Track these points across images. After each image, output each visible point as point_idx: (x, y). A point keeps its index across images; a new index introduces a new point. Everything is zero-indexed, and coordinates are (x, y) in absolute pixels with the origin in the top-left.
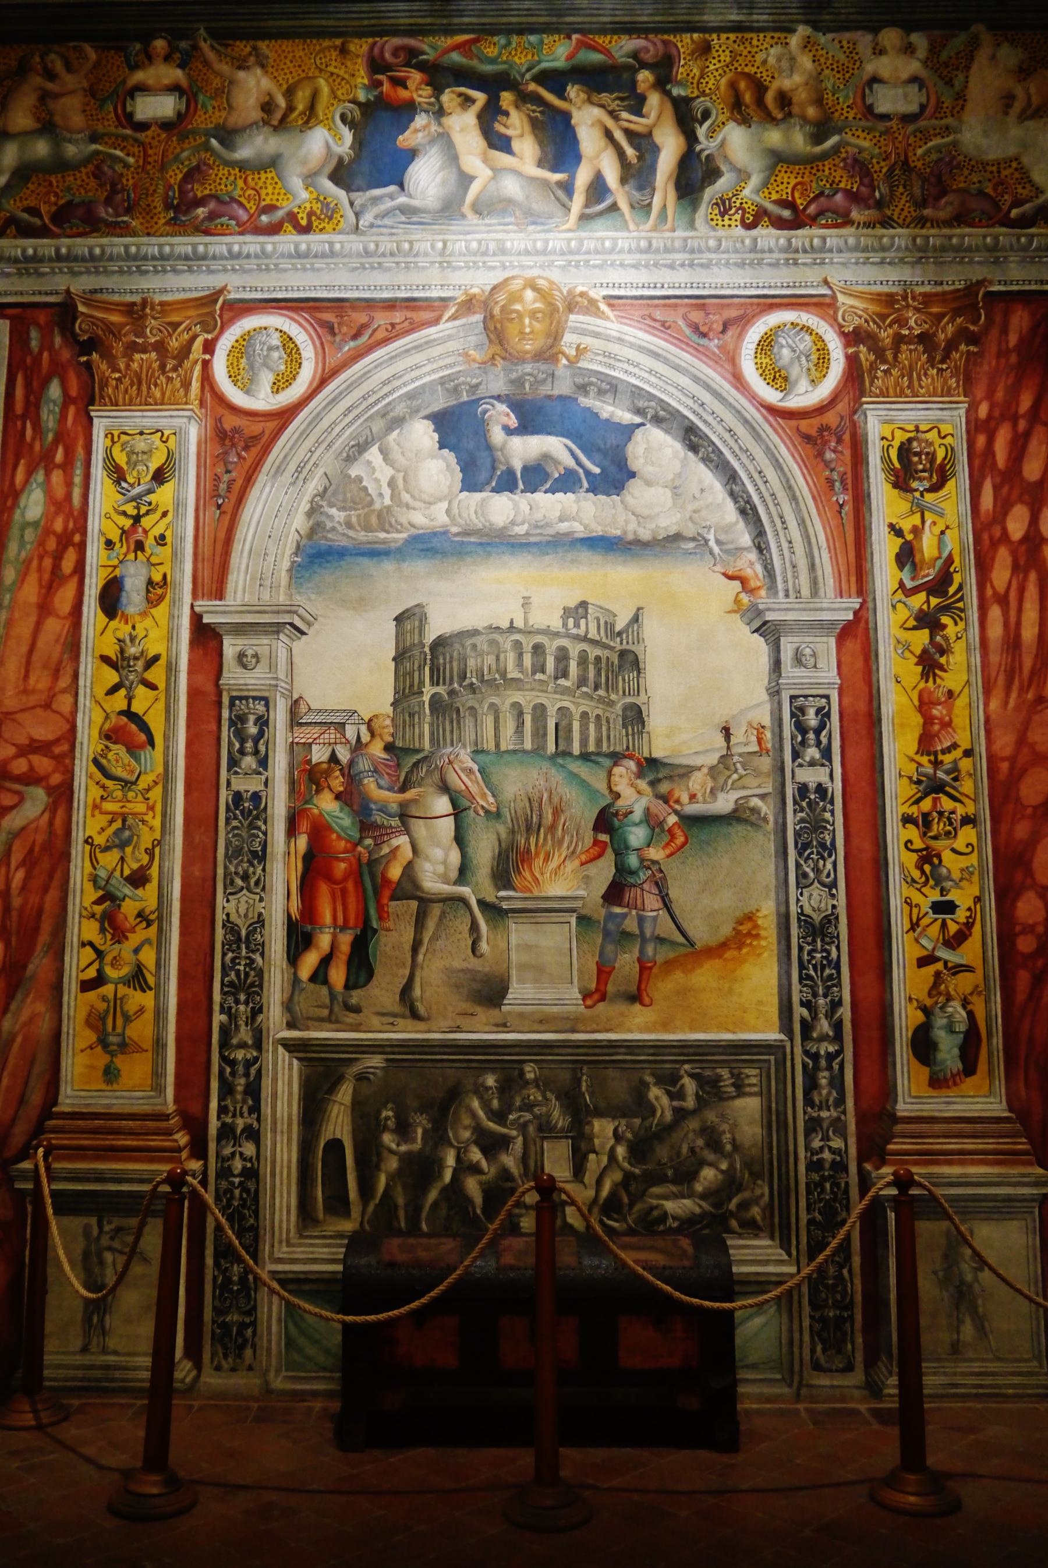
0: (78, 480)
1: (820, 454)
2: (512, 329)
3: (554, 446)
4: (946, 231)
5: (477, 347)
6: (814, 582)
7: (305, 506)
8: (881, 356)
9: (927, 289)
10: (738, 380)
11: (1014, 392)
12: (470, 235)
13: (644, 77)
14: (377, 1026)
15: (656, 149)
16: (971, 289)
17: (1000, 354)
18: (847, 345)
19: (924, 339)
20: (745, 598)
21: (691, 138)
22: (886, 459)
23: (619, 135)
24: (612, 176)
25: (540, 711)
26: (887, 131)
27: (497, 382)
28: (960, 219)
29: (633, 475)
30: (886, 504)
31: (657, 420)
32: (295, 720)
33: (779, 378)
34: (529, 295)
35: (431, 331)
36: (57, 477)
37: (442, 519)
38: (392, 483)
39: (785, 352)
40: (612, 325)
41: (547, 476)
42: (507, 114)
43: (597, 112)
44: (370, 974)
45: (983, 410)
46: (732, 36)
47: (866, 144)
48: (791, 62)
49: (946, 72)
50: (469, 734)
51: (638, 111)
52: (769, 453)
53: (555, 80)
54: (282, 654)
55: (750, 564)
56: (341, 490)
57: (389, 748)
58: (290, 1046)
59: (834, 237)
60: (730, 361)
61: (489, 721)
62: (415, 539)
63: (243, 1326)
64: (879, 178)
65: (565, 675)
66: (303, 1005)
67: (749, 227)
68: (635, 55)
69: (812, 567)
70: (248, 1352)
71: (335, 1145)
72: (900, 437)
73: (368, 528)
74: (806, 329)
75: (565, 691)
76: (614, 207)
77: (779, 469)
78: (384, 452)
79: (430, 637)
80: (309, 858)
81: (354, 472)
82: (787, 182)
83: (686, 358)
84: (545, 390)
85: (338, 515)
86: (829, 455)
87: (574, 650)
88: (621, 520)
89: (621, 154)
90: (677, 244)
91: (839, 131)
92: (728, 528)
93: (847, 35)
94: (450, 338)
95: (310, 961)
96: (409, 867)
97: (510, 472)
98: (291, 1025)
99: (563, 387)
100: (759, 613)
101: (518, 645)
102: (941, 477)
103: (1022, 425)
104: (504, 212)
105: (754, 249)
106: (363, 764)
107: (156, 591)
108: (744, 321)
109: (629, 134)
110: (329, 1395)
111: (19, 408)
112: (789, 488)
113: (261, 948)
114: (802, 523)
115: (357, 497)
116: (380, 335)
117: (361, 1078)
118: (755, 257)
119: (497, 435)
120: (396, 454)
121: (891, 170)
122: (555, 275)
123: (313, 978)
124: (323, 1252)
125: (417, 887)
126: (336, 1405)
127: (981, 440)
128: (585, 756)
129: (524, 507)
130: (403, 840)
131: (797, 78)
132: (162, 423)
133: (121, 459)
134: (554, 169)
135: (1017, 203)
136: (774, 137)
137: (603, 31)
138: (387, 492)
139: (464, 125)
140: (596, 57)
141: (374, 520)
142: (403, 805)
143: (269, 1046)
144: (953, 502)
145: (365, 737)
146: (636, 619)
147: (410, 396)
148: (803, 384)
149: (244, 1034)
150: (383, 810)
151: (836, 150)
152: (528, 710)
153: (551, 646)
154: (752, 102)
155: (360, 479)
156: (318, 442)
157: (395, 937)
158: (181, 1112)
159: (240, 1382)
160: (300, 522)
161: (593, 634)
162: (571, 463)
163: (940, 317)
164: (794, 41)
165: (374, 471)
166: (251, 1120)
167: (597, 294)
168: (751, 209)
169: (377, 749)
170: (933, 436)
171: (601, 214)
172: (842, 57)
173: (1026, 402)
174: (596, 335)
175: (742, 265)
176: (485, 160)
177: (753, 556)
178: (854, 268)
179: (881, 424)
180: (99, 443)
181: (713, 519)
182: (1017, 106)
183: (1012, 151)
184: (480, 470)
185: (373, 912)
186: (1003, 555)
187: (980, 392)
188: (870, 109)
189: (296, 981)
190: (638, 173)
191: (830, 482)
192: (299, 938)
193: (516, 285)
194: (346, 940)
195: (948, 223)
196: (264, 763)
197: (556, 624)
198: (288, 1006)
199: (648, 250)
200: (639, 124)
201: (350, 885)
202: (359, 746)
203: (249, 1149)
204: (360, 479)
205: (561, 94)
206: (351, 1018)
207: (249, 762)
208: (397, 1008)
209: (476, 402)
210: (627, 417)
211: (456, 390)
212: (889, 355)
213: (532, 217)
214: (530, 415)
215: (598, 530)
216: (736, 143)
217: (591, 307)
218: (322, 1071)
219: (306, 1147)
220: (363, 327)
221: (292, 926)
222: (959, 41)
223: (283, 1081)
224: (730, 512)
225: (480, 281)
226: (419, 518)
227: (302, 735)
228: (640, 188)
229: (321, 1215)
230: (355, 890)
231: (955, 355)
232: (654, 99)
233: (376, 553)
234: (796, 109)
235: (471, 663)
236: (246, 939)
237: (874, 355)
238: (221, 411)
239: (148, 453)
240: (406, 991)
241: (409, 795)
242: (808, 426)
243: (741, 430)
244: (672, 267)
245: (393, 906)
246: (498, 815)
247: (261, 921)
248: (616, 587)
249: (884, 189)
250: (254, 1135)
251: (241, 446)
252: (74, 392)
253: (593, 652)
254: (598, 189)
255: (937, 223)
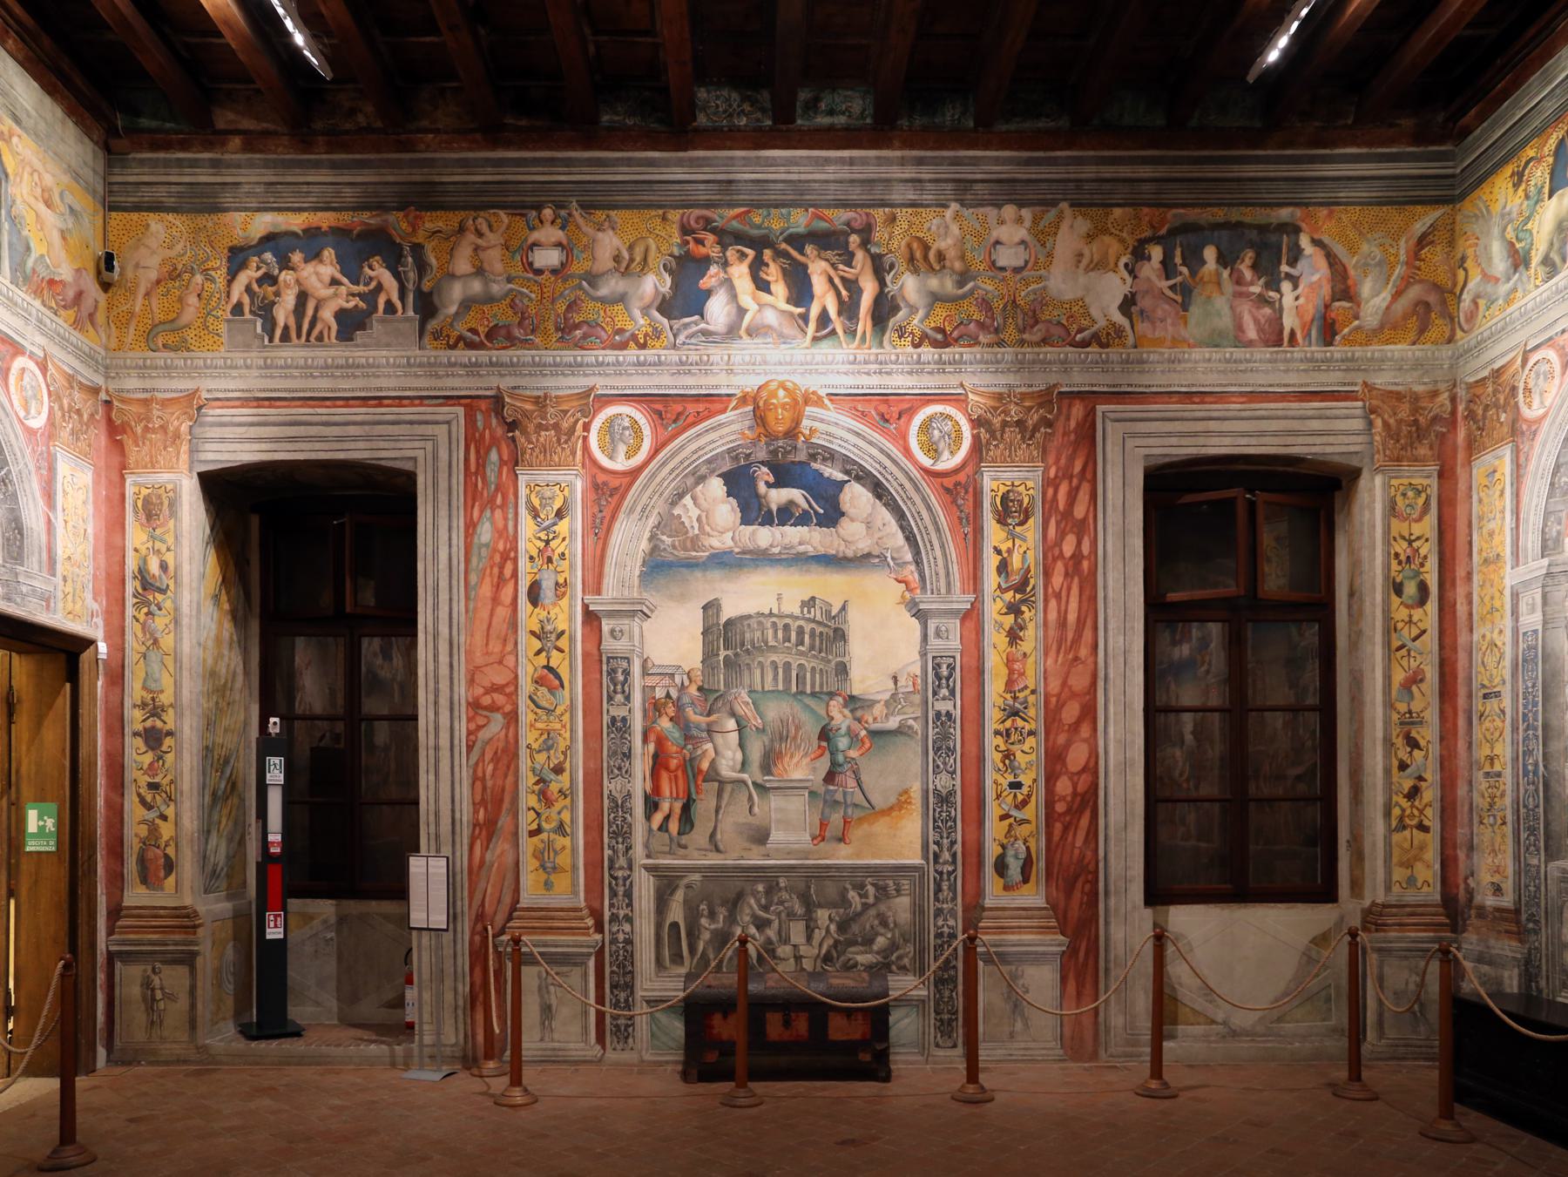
0: (511, 516)
1: (954, 501)
2: (770, 417)
3: (796, 494)
4: (1036, 350)
5: (750, 428)
6: (949, 584)
7: (647, 535)
8: (992, 434)
9: (1023, 389)
10: (907, 452)
11: (1071, 459)
12: (744, 350)
13: (854, 239)
14: (696, 856)
15: (860, 291)
16: (1049, 390)
17: (1064, 434)
18: (973, 428)
19: (1020, 423)
20: (908, 595)
21: (882, 283)
22: (993, 504)
23: (837, 281)
24: (832, 312)
25: (787, 666)
26: (1004, 279)
27: (762, 455)
28: (1045, 341)
29: (843, 514)
30: (994, 534)
31: (858, 479)
32: (645, 672)
33: (933, 450)
34: (781, 393)
35: (722, 418)
36: (498, 513)
37: (730, 543)
38: (699, 519)
39: (936, 432)
40: (831, 414)
41: (792, 515)
42: (767, 265)
43: (824, 264)
44: (692, 826)
45: (1052, 473)
46: (910, 210)
47: (990, 288)
48: (946, 228)
49: (1043, 235)
50: (746, 681)
51: (849, 264)
52: (924, 500)
53: (797, 241)
54: (636, 630)
55: (911, 572)
56: (669, 523)
57: (700, 689)
58: (648, 868)
59: (967, 353)
60: (901, 439)
61: (758, 672)
62: (713, 557)
63: (627, 1026)
64: (998, 312)
65: (802, 643)
66: (656, 845)
67: (916, 346)
68: (848, 224)
69: (948, 574)
70: (630, 1040)
71: (675, 925)
72: (1003, 489)
73: (685, 549)
74: (949, 417)
75: (802, 654)
76: (833, 332)
77: (930, 510)
78: (694, 499)
79: (723, 619)
80: (656, 757)
81: (676, 512)
82: (940, 316)
83: (876, 436)
84: (791, 457)
85: (668, 540)
86: (960, 502)
87: (808, 627)
88: (836, 544)
89: (838, 294)
90: (872, 358)
91: (974, 278)
92: (899, 550)
93: (982, 210)
94: (732, 422)
95: (658, 818)
96: (713, 762)
97: (770, 512)
98: (648, 856)
99: (802, 456)
100: (916, 604)
101: (774, 624)
102: (1026, 515)
103: (1075, 481)
104: (766, 334)
105: (918, 362)
106: (686, 700)
107: (561, 588)
108: (911, 412)
109: (843, 279)
110: (676, 1062)
111: (473, 468)
112: (935, 523)
113: (630, 811)
114: (942, 547)
115: (679, 528)
116: (690, 420)
117: (688, 887)
118: (918, 368)
119: (762, 488)
120: (701, 501)
121: (1005, 306)
122: (797, 379)
123: (660, 829)
124: (671, 985)
125: (718, 774)
126: (680, 1068)
127: (1050, 491)
128: (813, 694)
129: (778, 536)
130: (709, 746)
131: (950, 241)
132: (560, 478)
133: (536, 502)
134: (797, 305)
135: (1080, 331)
136: (933, 283)
137: (828, 206)
138: (696, 525)
139: (740, 273)
140: (824, 225)
141: (689, 544)
142: (709, 724)
143: (636, 868)
144: (1031, 531)
145: (686, 683)
146: (844, 608)
147: (709, 461)
148: (946, 454)
149: (622, 862)
150: (698, 727)
151: (971, 292)
152: (780, 665)
153: (794, 625)
154: (922, 258)
155: (679, 516)
156: (654, 492)
157: (705, 805)
158: (589, 907)
159: (626, 1056)
160: (644, 545)
161: (818, 618)
162: (806, 506)
163: (1030, 408)
164: (949, 213)
165: (688, 511)
166: (628, 911)
167: (823, 392)
168: (918, 333)
169: (693, 690)
170: (1022, 489)
171: (825, 337)
172: (977, 226)
173: (1078, 468)
174: (822, 421)
175: (910, 373)
176: (754, 299)
177: (913, 567)
178: (977, 377)
179: (992, 482)
180: (523, 491)
181: (890, 543)
182: (1085, 261)
183: (1079, 294)
184: (753, 511)
185: (693, 790)
186: (1060, 566)
187: (1051, 460)
188: (993, 263)
189: (650, 830)
190: (849, 309)
191: (960, 519)
192: (652, 805)
193: (773, 386)
194: (678, 806)
195: (1038, 344)
196: (628, 698)
197: (797, 612)
198: (646, 845)
199: (854, 362)
200: (851, 273)
201: (680, 773)
202: (683, 687)
203: (627, 927)
204: (679, 516)
205: (801, 251)
206: (682, 852)
207: (619, 698)
208: (708, 846)
209: (749, 466)
210: (840, 476)
211: (736, 458)
212: (998, 434)
213: (783, 338)
214: (783, 473)
215: (822, 551)
216: (909, 286)
217: (819, 402)
218: (667, 883)
219: (659, 926)
220: (679, 414)
221: (647, 797)
222: (1053, 212)
223: (645, 888)
224: (900, 539)
225: (750, 383)
226: (715, 543)
227: (650, 681)
228: (850, 319)
229: (667, 963)
230: (683, 779)
231: (1038, 435)
232: (860, 256)
233: (691, 565)
234: (948, 263)
235: (747, 636)
236: (621, 806)
237: (989, 435)
238: (595, 470)
239: (552, 498)
240: (713, 836)
241: (712, 718)
242: (949, 482)
243: (908, 485)
244: (868, 374)
245: (705, 786)
246: (764, 730)
247: (629, 795)
248: (832, 587)
249: (1000, 320)
250: (629, 919)
251: (609, 493)
252: (505, 458)
253: (819, 629)
254: (824, 319)
255: (1031, 344)
